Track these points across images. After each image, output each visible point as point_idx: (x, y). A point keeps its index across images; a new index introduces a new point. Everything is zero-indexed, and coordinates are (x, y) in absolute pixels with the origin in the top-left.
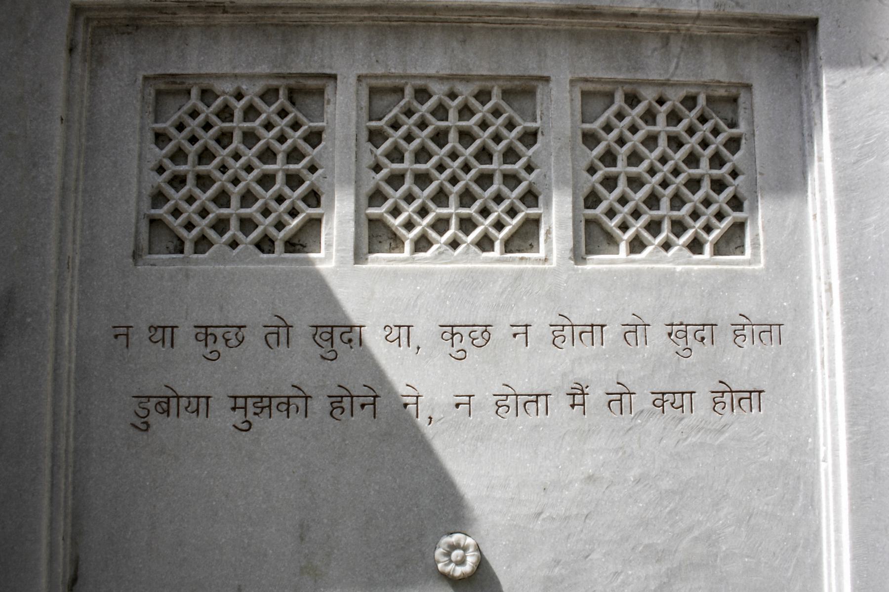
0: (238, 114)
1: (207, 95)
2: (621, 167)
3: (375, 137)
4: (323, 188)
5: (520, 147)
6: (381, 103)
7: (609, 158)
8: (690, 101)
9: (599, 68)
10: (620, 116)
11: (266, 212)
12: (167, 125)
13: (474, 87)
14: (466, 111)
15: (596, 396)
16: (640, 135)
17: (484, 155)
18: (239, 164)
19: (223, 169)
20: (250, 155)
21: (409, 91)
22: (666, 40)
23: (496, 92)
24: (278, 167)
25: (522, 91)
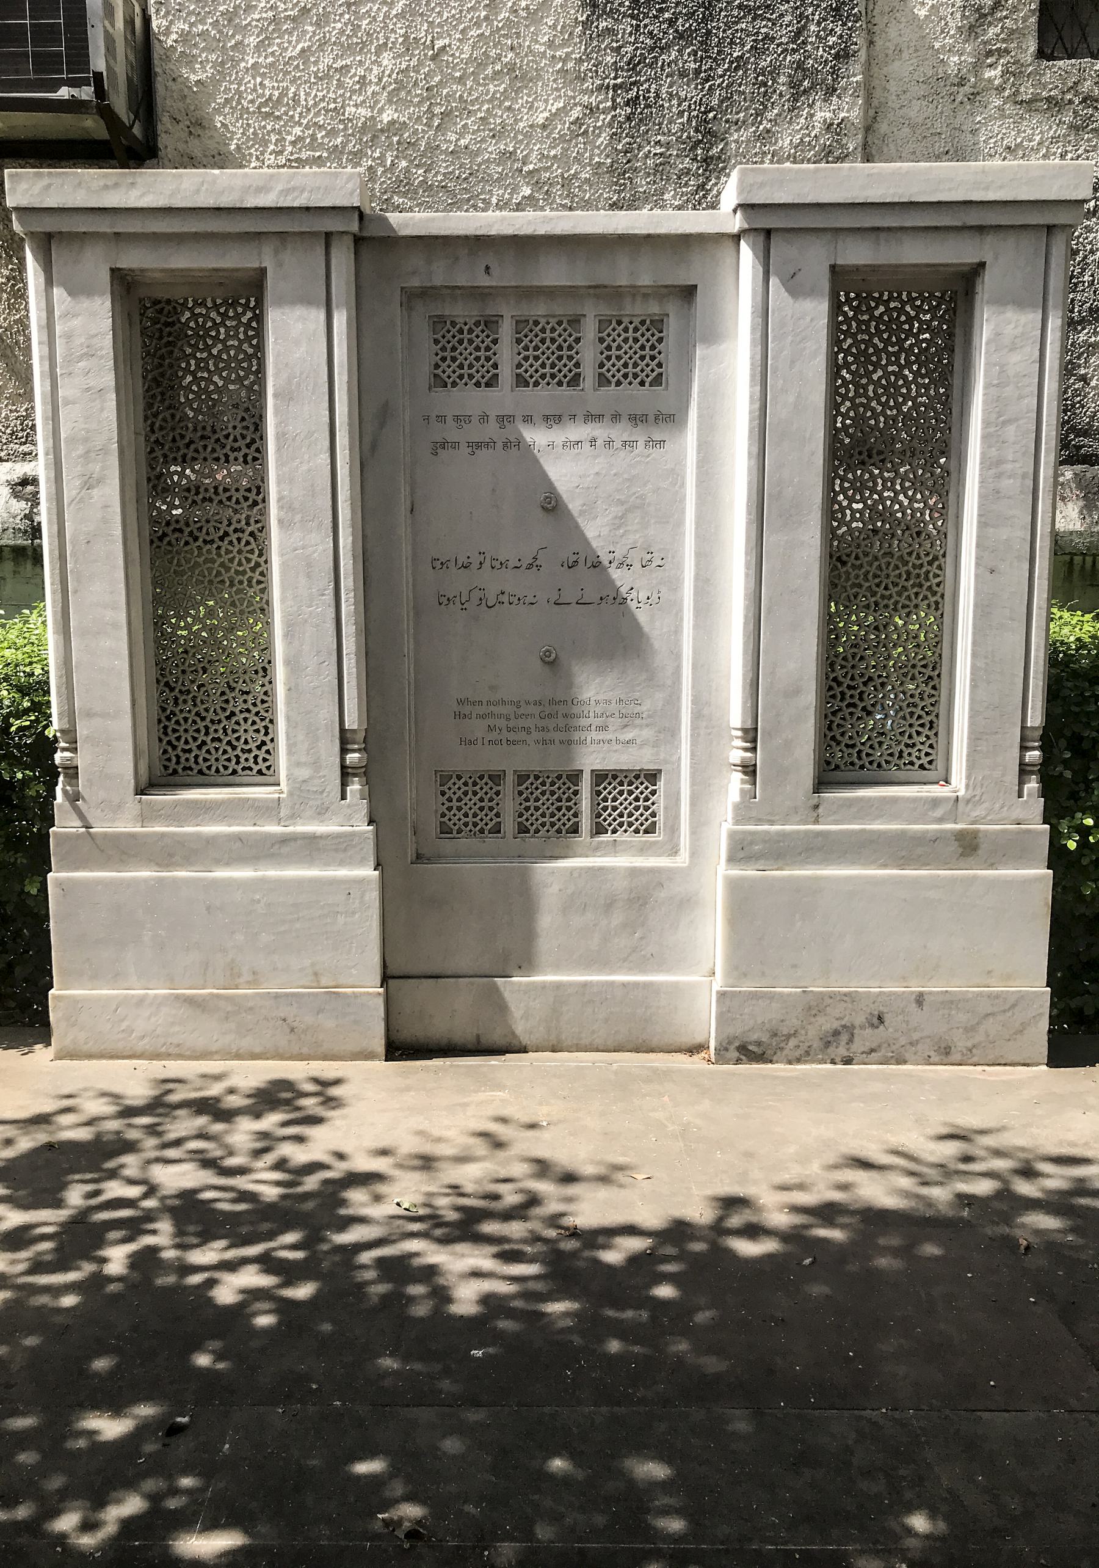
0: (465, 332)
1: (454, 324)
2: (614, 352)
3: (519, 341)
4: (499, 363)
5: (574, 344)
6: (522, 325)
7: (609, 348)
8: (643, 323)
9: (607, 311)
10: (614, 330)
11: (478, 372)
12: (438, 336)
13: (556, 320)
14: (553, 330)
15: (599, 442)
16: (622, 338)
17: (560, 348)
18: (466, 352)
19: (461, 354)
20: (471, 349)
21: (531, 322)
22: (634, 295)
23: (565, 322)
24: (482, 353)
25: (575, 321)
